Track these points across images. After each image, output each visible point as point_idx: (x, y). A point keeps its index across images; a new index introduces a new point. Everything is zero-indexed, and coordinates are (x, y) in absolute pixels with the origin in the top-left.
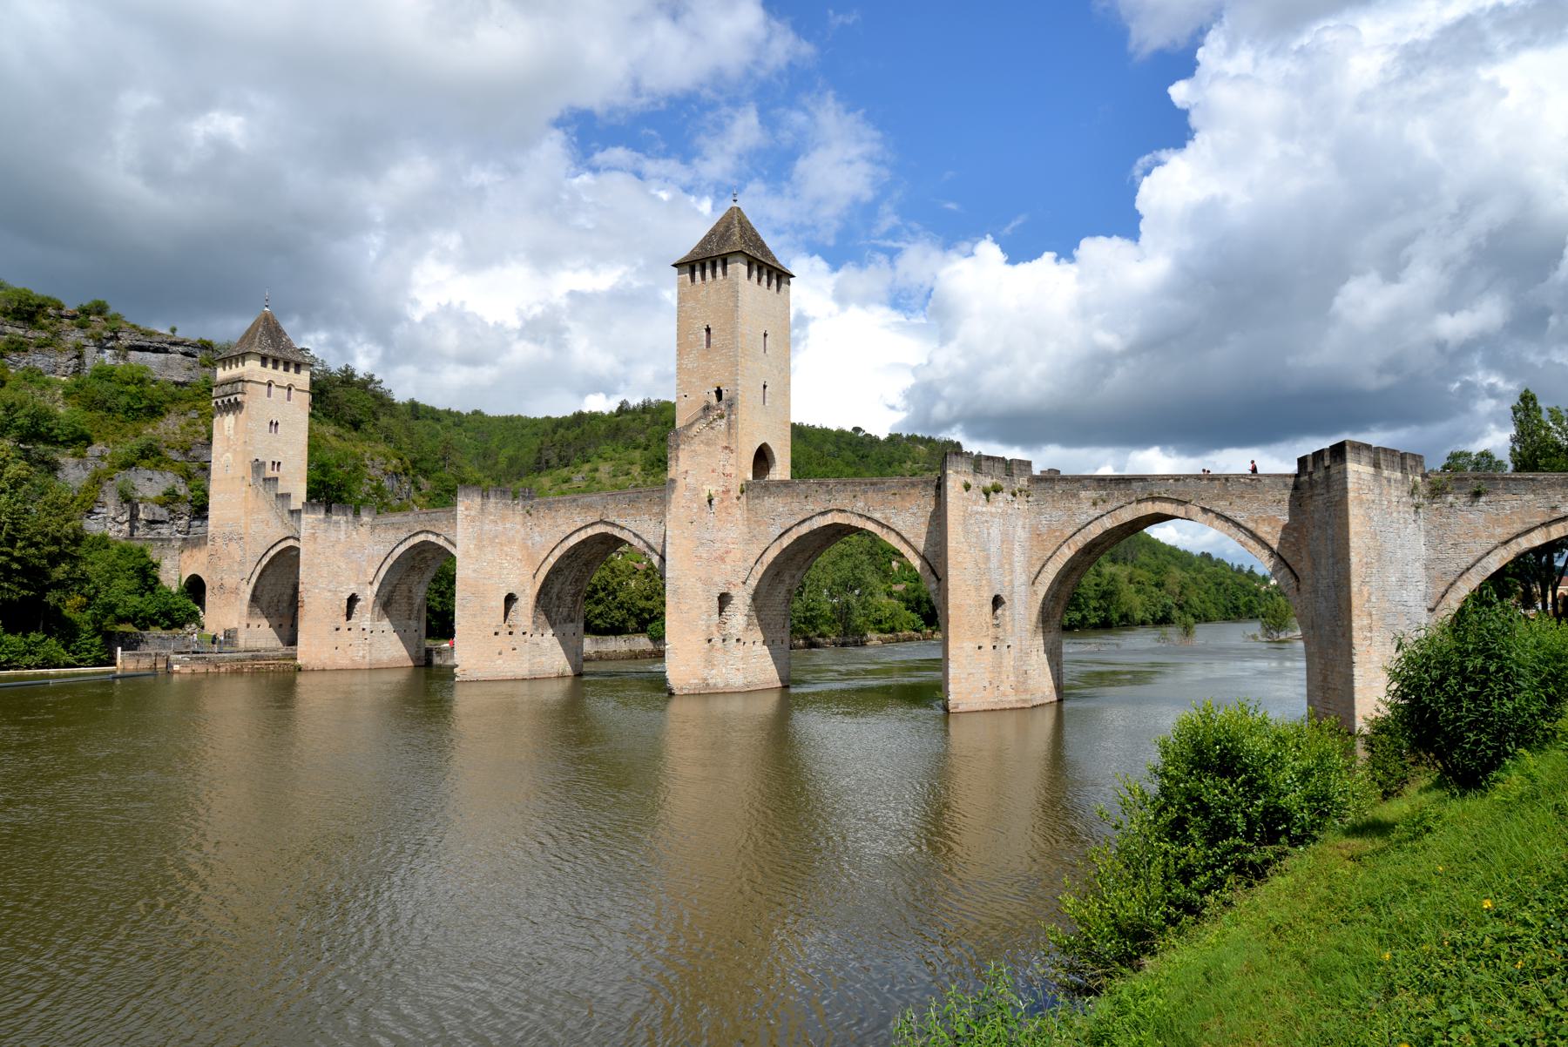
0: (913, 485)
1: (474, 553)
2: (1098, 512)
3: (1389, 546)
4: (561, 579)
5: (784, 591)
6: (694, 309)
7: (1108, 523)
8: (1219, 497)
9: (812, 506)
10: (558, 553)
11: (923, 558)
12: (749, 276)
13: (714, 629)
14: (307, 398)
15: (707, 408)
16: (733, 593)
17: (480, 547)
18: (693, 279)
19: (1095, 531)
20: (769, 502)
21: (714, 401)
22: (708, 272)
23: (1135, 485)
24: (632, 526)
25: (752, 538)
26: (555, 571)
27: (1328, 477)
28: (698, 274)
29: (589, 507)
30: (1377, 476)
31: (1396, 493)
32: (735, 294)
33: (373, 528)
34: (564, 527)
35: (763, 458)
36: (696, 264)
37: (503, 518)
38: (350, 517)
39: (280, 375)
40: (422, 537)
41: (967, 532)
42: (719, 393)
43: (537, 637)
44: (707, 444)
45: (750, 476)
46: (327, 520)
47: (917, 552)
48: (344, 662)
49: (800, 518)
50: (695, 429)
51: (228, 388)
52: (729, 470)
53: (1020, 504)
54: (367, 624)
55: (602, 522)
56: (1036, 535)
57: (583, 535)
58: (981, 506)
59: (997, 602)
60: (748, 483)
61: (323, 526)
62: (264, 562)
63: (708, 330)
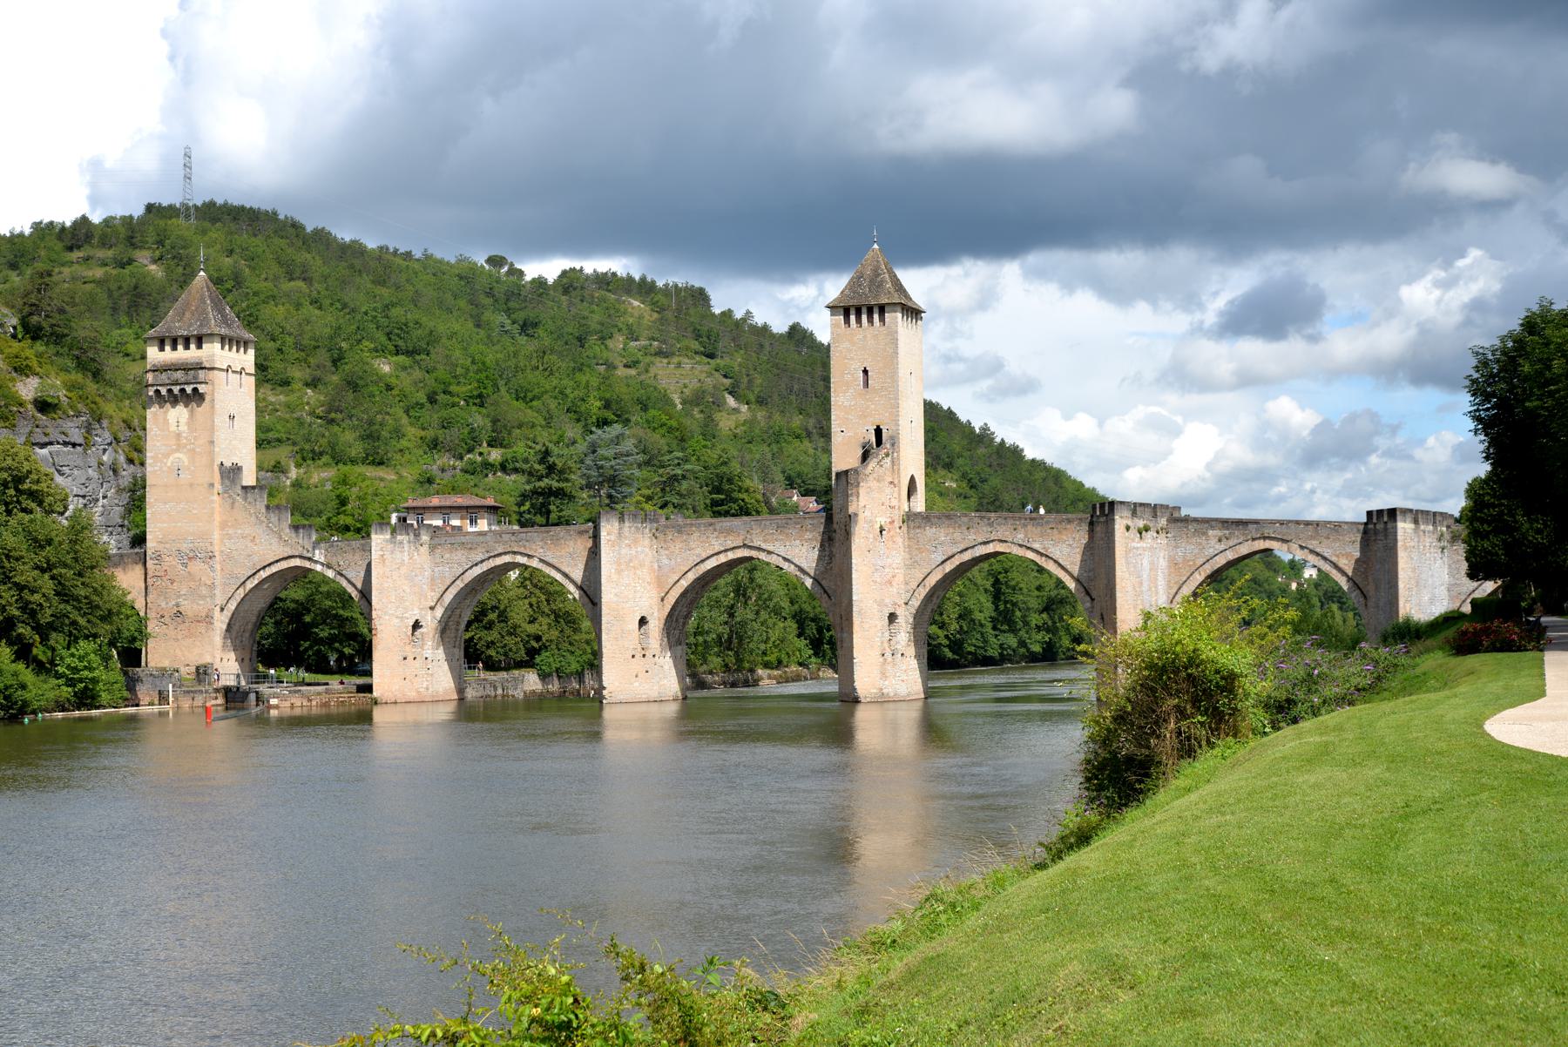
0: (1069, 521)
1: (615, 577)
2: (1223, 547)
3: (1424, 576)
6: (850, 351)
7: (1230, 555)
8: (1312, 538)
9: (972, 537)
10: (691, 576)
11: (1077, 580)
17: (619, 572)
18: (847, 321)
19: (1220, 561)
22: (864, 317)
23: (1251, 526)
25: (912, 564)
27: (1386, 529)
28: (853, 318)
29: (729, 531)
30: (1416, 530)
31: (1429, 541)
33: (433, 548)
34: (698, 551)
37: (636, 541)
41: (1128, 563)
42: (878, 431)
47: (1072, 576)
48: (412, 695)
49: (962, 547)
51: (179, 375)
52: (894, 502)
53: (1162, 540)
55: (745, 546)
56: (1174, 564)
58: (1137, 544)
61: (390, 546)
62: (250, 585)
63: (865, 372)
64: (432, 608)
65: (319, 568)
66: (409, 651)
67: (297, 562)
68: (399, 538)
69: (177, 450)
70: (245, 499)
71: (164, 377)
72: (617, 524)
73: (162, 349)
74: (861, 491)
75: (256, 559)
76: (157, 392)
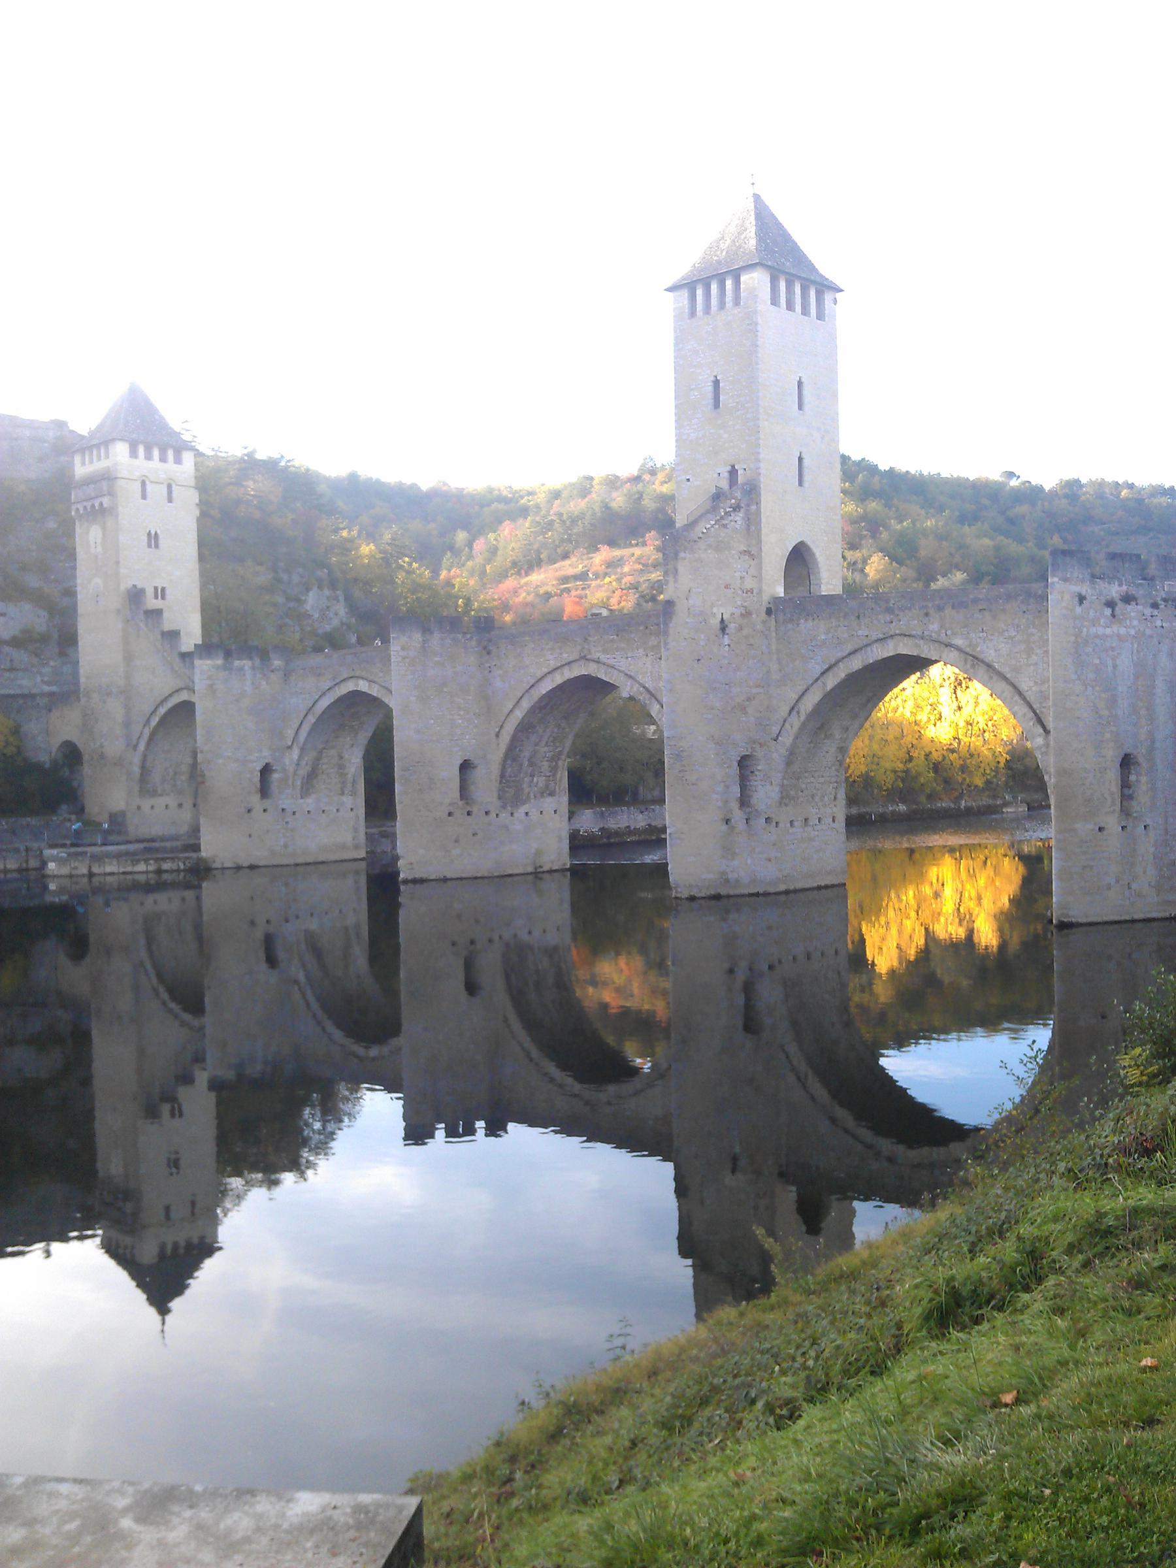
0: (1009, 597)
4: (534, 738)
5: (833, 750)
10: (526, 704)
12: (775, 301)
13: (735, 805)
14: (193, 497)
15: (718, 496)
16: (760, 753)
18: (693, 313)
20: (806, 625)
21: (724, 484)
24: (623, 664)
26: (525, 727)
32: (752, 329)
35: (799, 559)
36: (707, 285)
38: (257, 661)
39: (154, 467)
40: (350, 686)
42: (733, 472)
43: (504, 815)
44: (719, 547)
45: (780, 591)
46: (226, 667)
48: (259, 855)
49: (849, 648)
50: (701, 527)
51: (90, 490)
52: (749, 584)
54: (286, 802)
55: (584, 658)
57: (558, 679)
59: (1127, 762)
60: (776, 600)
62: (154, 721)
63: (716, 383)
64: (290, 747)
66: (255, 799)
68: (237, 663)
70: (147, 625)
72: (418, 636)
74: (681, 569)
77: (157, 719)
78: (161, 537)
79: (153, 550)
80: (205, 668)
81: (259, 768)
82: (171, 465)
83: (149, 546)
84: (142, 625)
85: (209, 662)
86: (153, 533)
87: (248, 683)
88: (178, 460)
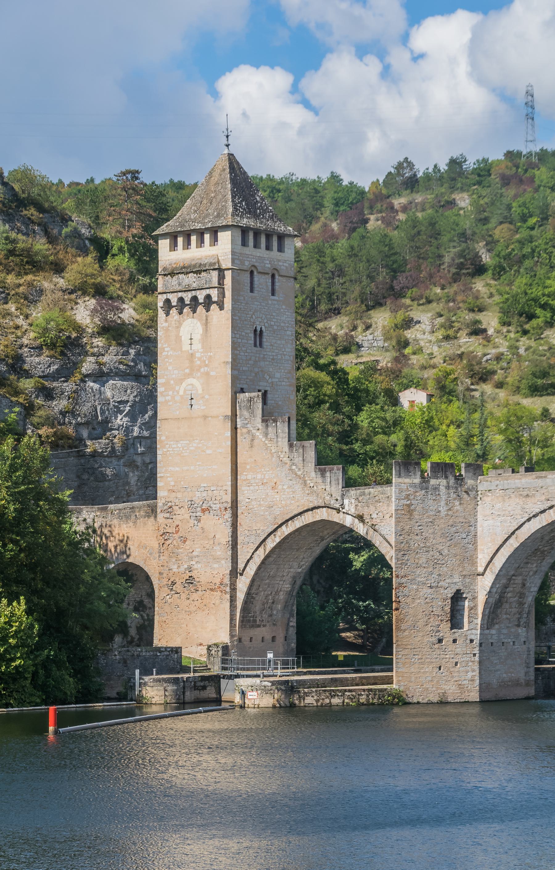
38: (452, 481)
51: (190, 280)
62: (271, 544)
65: (348, 521)
67: (322, 514)
68: (433, 482)
69: (190, 375)
70: (266, 435)
71: (173, 282)
73: (174, 246)
75: (277, 511)
76: (168, 301)
77: (278, 540)
78: (265, 334)
79: (259, 349)
80: (404, 487)
81: (450, 596)
82: (275, 253)
83: (255, 345)
84: (259, 435)
85: (407, 480)
86: (259, 329)
87: (443, 503)
88: (281, 249)
